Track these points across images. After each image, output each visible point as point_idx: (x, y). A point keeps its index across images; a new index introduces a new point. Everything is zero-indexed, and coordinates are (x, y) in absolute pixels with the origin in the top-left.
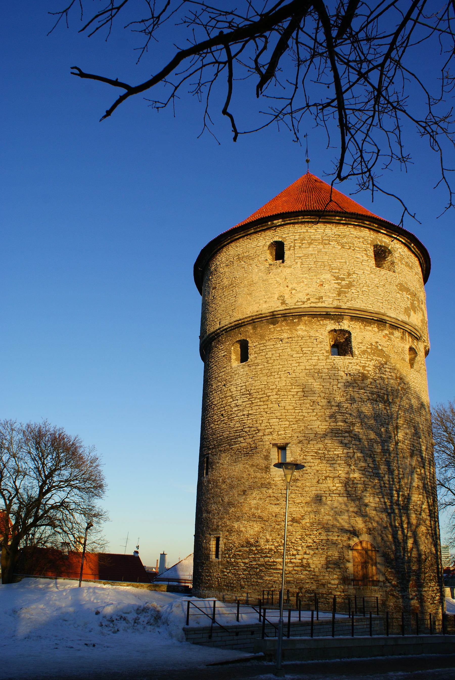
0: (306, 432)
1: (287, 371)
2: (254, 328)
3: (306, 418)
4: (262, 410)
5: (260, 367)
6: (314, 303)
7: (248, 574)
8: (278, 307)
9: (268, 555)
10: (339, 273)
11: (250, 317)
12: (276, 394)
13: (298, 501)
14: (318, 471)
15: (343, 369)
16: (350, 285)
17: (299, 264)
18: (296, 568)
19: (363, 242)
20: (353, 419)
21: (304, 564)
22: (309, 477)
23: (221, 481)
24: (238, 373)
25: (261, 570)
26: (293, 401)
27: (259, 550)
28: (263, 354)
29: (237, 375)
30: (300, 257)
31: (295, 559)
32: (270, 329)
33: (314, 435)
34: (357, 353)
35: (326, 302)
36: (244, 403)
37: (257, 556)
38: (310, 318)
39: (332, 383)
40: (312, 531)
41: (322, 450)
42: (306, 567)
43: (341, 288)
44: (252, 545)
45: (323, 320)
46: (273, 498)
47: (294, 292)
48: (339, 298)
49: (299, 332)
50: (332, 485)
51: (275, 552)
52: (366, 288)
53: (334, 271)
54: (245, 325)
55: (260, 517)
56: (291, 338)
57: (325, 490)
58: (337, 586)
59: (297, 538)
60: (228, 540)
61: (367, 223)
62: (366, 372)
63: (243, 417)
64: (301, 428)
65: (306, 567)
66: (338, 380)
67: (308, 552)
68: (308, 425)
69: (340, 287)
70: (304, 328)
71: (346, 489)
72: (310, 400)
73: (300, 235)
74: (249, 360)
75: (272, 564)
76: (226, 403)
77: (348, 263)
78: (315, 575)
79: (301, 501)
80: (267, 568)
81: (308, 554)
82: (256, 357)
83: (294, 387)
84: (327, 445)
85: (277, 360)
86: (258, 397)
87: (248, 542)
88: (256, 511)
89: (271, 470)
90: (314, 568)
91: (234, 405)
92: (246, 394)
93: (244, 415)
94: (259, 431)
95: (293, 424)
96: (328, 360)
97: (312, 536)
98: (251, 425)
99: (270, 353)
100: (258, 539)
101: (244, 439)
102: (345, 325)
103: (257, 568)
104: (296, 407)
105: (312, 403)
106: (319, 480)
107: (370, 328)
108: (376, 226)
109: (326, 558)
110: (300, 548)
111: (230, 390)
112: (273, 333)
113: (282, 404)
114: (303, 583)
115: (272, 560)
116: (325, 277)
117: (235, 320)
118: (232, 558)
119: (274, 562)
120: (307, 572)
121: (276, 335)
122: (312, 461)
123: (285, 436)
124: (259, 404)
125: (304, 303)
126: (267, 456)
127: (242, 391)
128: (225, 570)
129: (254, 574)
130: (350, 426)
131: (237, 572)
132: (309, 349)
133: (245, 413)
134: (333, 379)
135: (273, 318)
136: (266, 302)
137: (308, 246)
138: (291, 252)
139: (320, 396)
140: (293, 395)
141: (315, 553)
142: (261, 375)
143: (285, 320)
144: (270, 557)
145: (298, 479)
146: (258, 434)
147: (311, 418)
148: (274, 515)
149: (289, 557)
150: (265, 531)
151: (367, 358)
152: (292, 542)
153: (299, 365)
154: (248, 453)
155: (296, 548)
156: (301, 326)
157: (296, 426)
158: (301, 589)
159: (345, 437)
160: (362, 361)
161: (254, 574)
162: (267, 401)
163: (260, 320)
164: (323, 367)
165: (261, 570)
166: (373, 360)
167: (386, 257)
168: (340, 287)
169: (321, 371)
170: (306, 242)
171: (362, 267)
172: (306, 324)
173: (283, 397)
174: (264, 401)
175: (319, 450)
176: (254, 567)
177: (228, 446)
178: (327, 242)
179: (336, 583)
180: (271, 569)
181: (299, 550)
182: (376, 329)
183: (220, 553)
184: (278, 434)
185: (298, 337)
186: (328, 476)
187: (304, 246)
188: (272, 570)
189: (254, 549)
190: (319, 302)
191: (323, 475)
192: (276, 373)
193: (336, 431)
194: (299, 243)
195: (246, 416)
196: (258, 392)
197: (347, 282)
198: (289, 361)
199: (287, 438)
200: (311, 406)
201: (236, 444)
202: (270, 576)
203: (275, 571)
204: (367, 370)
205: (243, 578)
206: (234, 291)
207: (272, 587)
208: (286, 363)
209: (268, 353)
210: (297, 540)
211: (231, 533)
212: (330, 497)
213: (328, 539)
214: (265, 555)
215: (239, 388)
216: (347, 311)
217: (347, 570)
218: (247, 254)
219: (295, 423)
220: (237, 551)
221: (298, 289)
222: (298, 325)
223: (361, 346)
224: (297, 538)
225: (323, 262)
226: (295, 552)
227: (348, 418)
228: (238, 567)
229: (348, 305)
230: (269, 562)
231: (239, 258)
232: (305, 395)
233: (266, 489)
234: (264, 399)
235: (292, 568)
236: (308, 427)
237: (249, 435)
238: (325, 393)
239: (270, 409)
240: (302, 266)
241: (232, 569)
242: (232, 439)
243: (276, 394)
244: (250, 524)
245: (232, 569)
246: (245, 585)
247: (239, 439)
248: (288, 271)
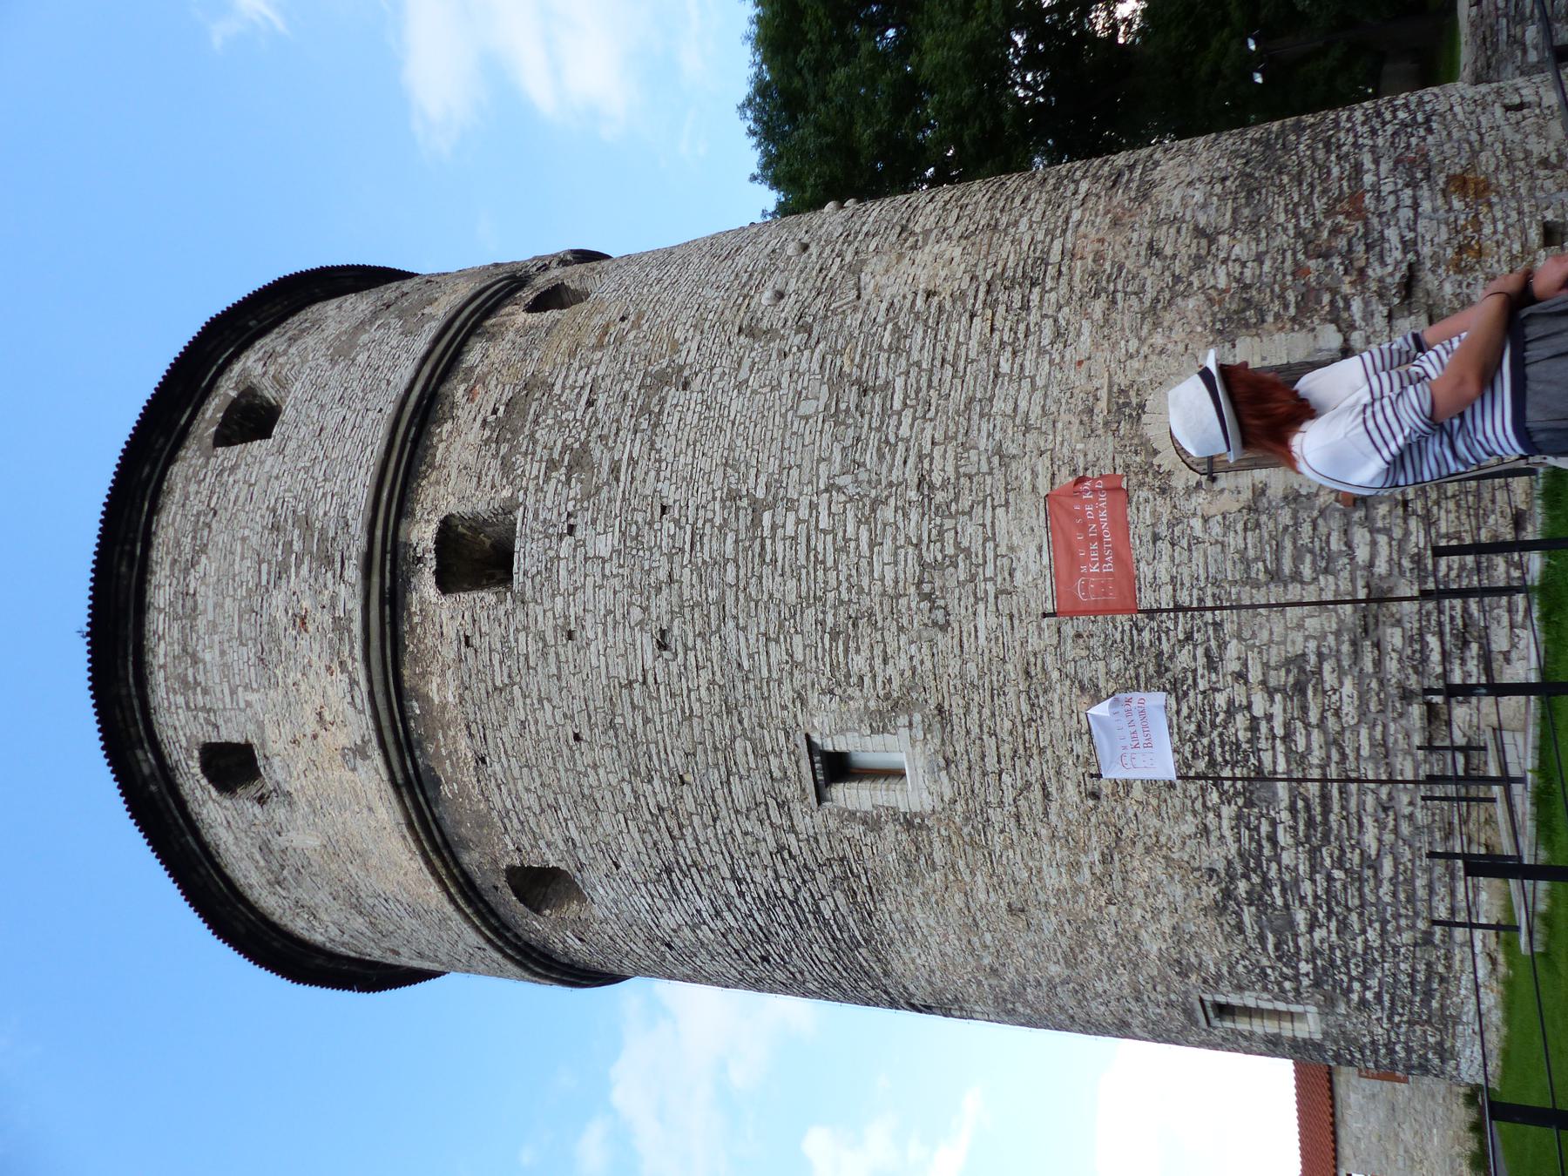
0: (765, 673)
1: (572, 742)
3: (718, 674)
4: (710, 832)
5: (574, 834)
6: (352, 647)
7: (1361, 915)
8: (377, 771)
9: (1265, 828)
10: (269, 563)
11: (428, 862)
12: (650, 782)
13: (1025, 708)
14: (901, 629)
15: (554, 539)
16: (306, 523)
17: (253, 697)
18: (1313, 717)
19: (199, 483)
20: (714, 499)
21: (1291, 680)
22: (928, 664)
25: (1340, 863)
26: (666, 721)
27: (1247, 866)
28: (532, 820)
29: (622, 906)
30: (233, 692)
31: (1269, 718)
33: (772, 645)
34: (506, 493)
35: (349, 606)
37: (1273, 874)
38: (407, 658)
39: (599, 582)
40: (1141, 647)
41: (824, 612)
42: (1302, 670)
43: (311, 553)
44: (1228, 894)
45: (410, 615)
46: (1022, 802)
47: (328, 717)
48: (338, 558)
49: (451, 699)
50: (952, 569)
51: (1249, 804)
52: (317, 467)
53: (264, 582)
54: (464, 873)
55: (1106, 859)
56: (468, 727)
57: (972, 600)
58: (1379, 531)
59: (1178, 712)
60: (1219, 977)
61: (147, 470)
62: (567, 458)
63: (748, 899)
64: (752, 692)
65: (1302, 670)
66: (586, 559)
67: (1235, 666)
68: (739, 665)
69: (307, 559)
70: (436, 680)
71: (963, 513)
72: (655, 659)
73: (175, 693)
74: (563, 866)
75: (1302, 816)
77: (247, 532)
78: (1338, 634)
79: (1023, 696)
80: (1326, 839)
81: (1245, 665)
82: (548, 845)
83: (619, 720)
84: (804, 594)
85: (541, 776)
86: (669, 843)
87: (1220, 908)
88: (1086, 870)
89: (916, 808)
90: (1307, 638)
91: (719, 923)
92: (671, 881)
94: (783, 848)
95: (741, 722)
96: (529, 593)
97: (1165, 647)
98: (770, 873)
99: (525, 796)
100: (1199, 869)
101: (823, 897)
102: (423, 534)
103: (1330, 878)
104: (683, 712)
105: (666, 654)
106: (935, 624)
107: (441, 446)
108: (161, 441)
109: (1257, 585)
110: (1221, 700)
112: (463, 786)
113: (677, 760)
114: (1381, 683)
115: (1285, 816)
116: (281, 608)
118: (1296, 968)
119: (1293, 809)
120: (1327, 667)
121: (469, 778)
122: (865, 653)
123: (785, 756)
124: (692, 845)
125: (353, 683)
126: (865, 822)
127: (666, 896)
128: (1355, 997)
129: (1360, 890)
130: (738, 509)
131: (1355, 954)
132: (496, 663)
133: (733, 892)
134: (586, 576)
135: (414, 785)
136: (370, 809)
137: (201, 666)
138: (220, 722)
139: (641, 622)
140: (646, 721)
141: (1240, 638)
142: (600, 830)
143: (420, 743)
144: (1274, 823)
145: (940, 708)
146: (795, 851)
147: (715, 657)
148: (1091, 803)
149: (1263, 744)
150: (1163, 840)
151: (526, 454)
152: (1200, 731)
153: (550, 700)
154: (870, 888)
155: (1222, 716)
156: (433, 689)
157: (745, 714)
158: (1406, 696)
159: (774, 527)
160: (535, 473)
161: (1360, 890)
162: (675, 813)
163: (433, 827)
164: (550, 614)
165: (1340, 863)
166: (532, 434)
167: (268, 401)
168: (307, 559)
169: (560, 622)
170: (190, 672)
171: (263, 482)
172: (423, 675)
173: (655, 757)
174: (681, 826)
175: (823, 623)
176: (1328, 891)
178: (189, 603)
179: (1368, 535)
180: (1326, 821)
181: (1231, 702)
182: (448, 426)
183: (1281, 1006)
184: (781, 780)
185: (462, 698)
186: (919, 585)
187: (201, 678)
188: (1332, 817)
189: (1242, 886)
190: (350, 631)
191: (913, 605)
192: (584, 781)
193: (757, 560)
194: (195, 694)
195: (744, 887)
196: (655, 844)
197: (297, 532)
198: (538, 733)
199: (792, 747)
200: (676, 654)
202: (1361, 824)
203: (1336, 807)
204: (565, 448)
205: (1383, 932)
206: (370, 901)
207: (1411, 817)
208: (545, 744)
209: (526, 804)
210: (1185, 711)
211: (1190, 964)
212: (999, 579)
213: (1172, 578)
214: (1264, 843)
215: (660, 903)
216: (379, 533)
217: (1303, 492)
218: (258, 856)
219: (735, 719)
220: (1264, 949)
221: (318, 701)
222: (425, 699)
223: (489, 478)
224: (1178, 712)
225: (240, 617)
226: (1241, 720)
227: (710, 515)
228: (1332, 948)
229: (358, 527)
230: (1295, 828)
232: (640, 679)
233: (990, 831)
234: (673, 824)
235: (1315, 733)
236: (746, 665)
237: (804, 882)
238: (630, 604)
239: (702, 805)
240: (255, 686)
241: (1348, 973)
242: (834, 938)
243: (650, 782)
244: (1141, 896)
245: (1348, 973)
246: (1413, 927)
247: (827, 914)
248: (271, 732)
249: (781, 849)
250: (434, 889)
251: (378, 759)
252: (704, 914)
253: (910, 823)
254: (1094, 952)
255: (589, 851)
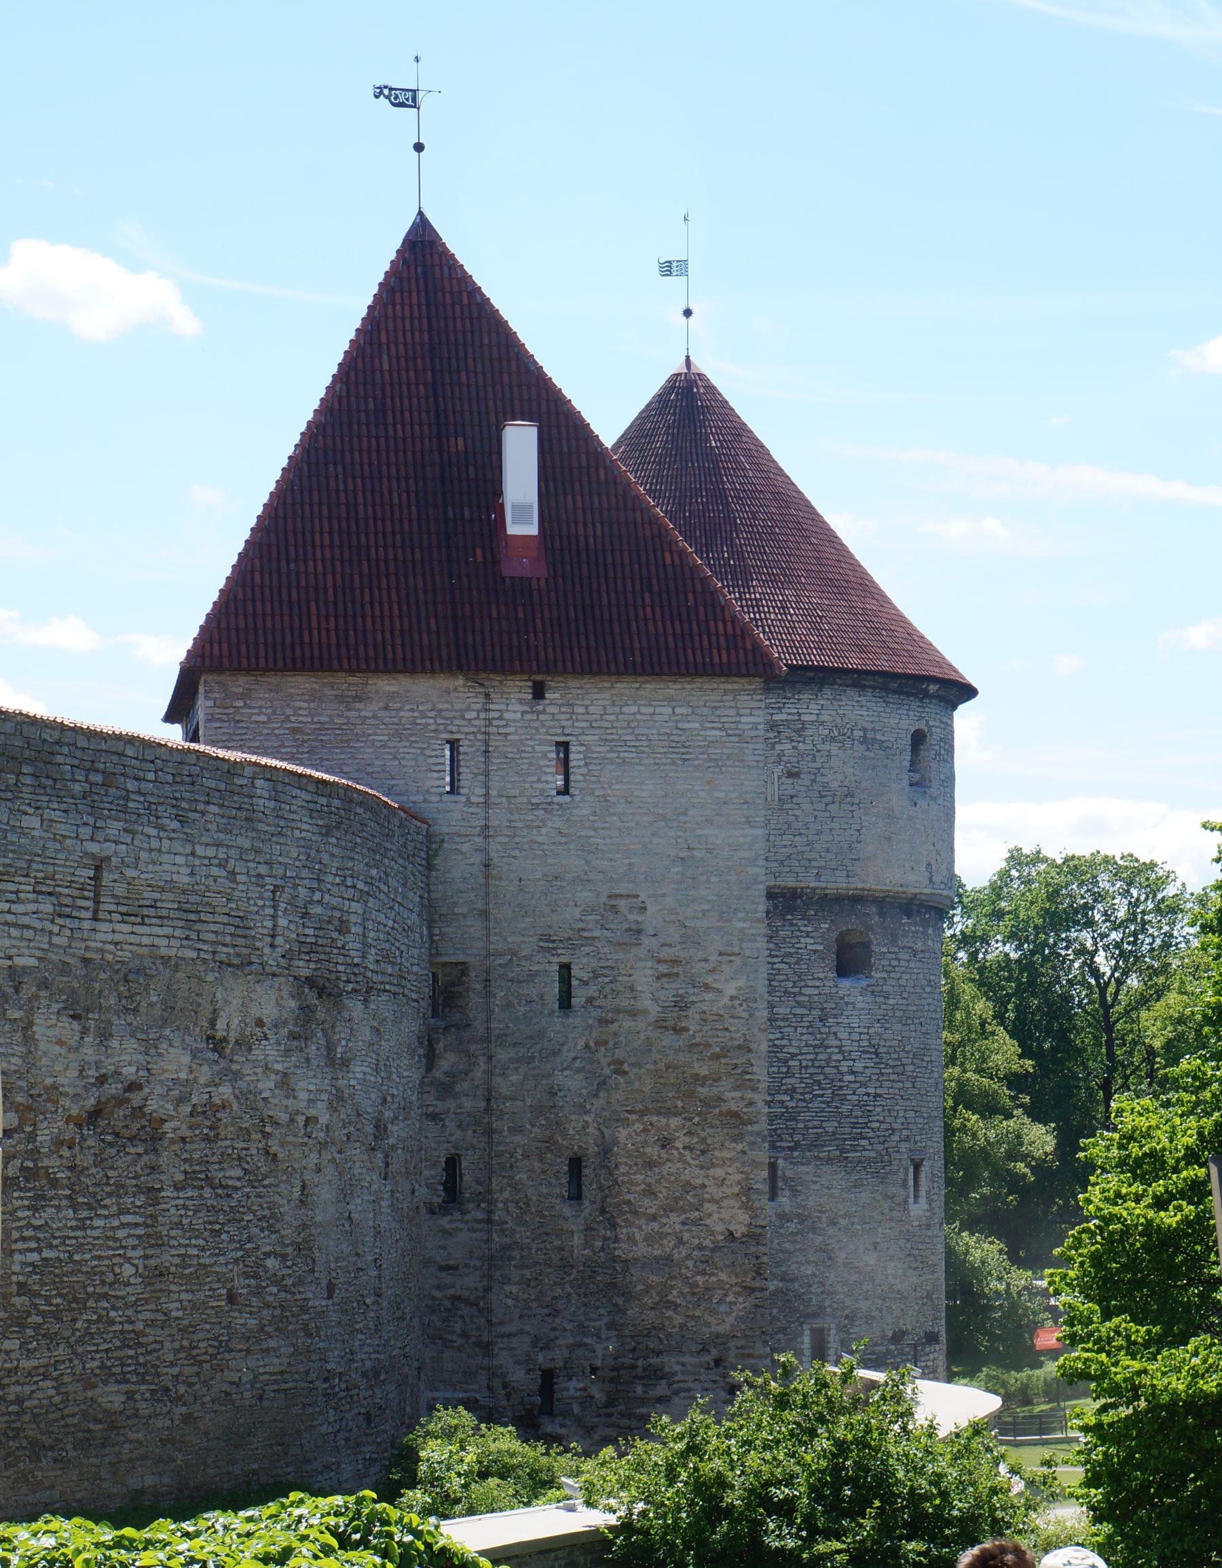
2: (882, 914)
23: (824, 1219)
24: (853, 1003)
29: (850, 1007)
32: (904, 925)
36: (867, 1071)
63: (865, 1098)
76: (828, 1060)
86: (891, 1063)
91: (846, 1069)
93: (868, 1094)
111: (835, 1034)
117: (859, 886)
121: (908, 942)
177: (838, 1153)
201: (856, 1151)
231: (865, 736)
242: (845, 1139)
247: (862, 1142)
249: (893, 1130)
250: (870, 884)
251: (928, 891)
252: (851, 1063)
253: (906, 1202)
254: (855, 1277)
255: (883, 1007)
